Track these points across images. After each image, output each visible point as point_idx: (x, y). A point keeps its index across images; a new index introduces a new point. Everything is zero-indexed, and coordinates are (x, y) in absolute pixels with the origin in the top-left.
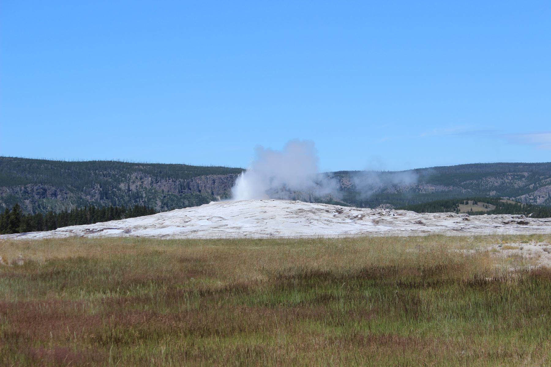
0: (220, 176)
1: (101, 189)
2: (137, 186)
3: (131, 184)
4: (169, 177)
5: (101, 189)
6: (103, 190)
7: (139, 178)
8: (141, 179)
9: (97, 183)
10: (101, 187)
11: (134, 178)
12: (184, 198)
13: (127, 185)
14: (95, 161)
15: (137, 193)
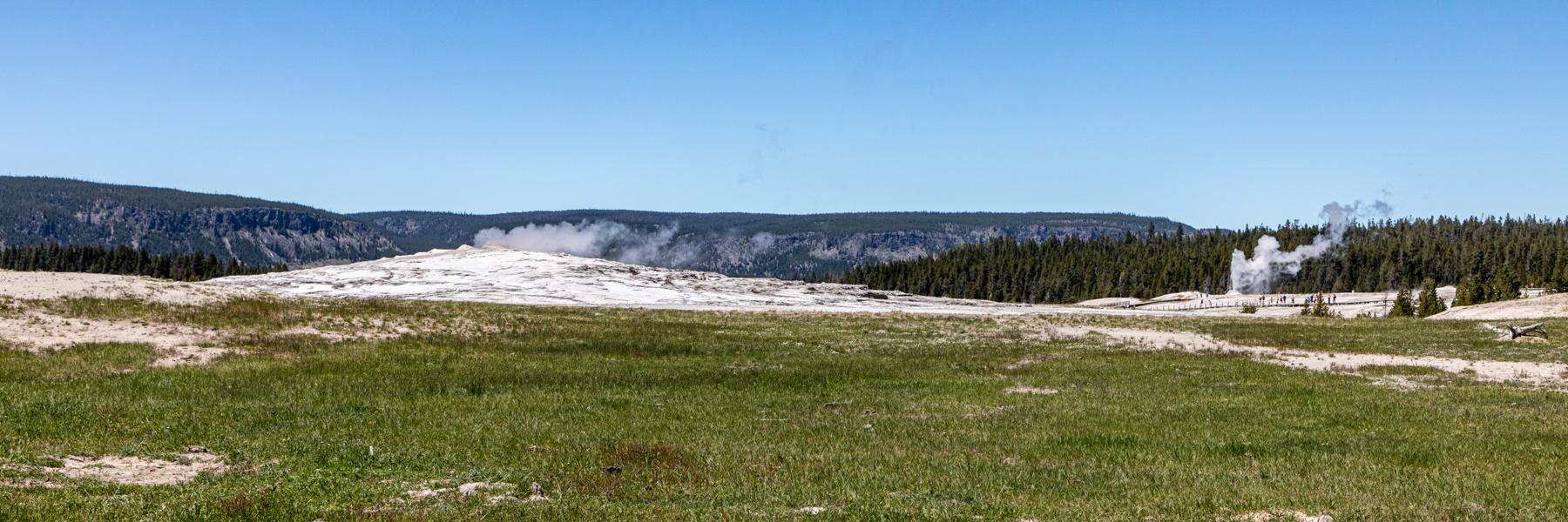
0: (228, 209)
1: (46, 220)
2: (101, 218)
3: (92, 214)
4: (152, 208)
5: (46, 220)
6: (49, 221)
7: (105, 206)
8: (110, 207)
9: (40, 210)
10: (45, 217)
11: (97, 206)
12: (175, 239)
13: (86, 216)
14: (38, 177)
15: (103, 228)
